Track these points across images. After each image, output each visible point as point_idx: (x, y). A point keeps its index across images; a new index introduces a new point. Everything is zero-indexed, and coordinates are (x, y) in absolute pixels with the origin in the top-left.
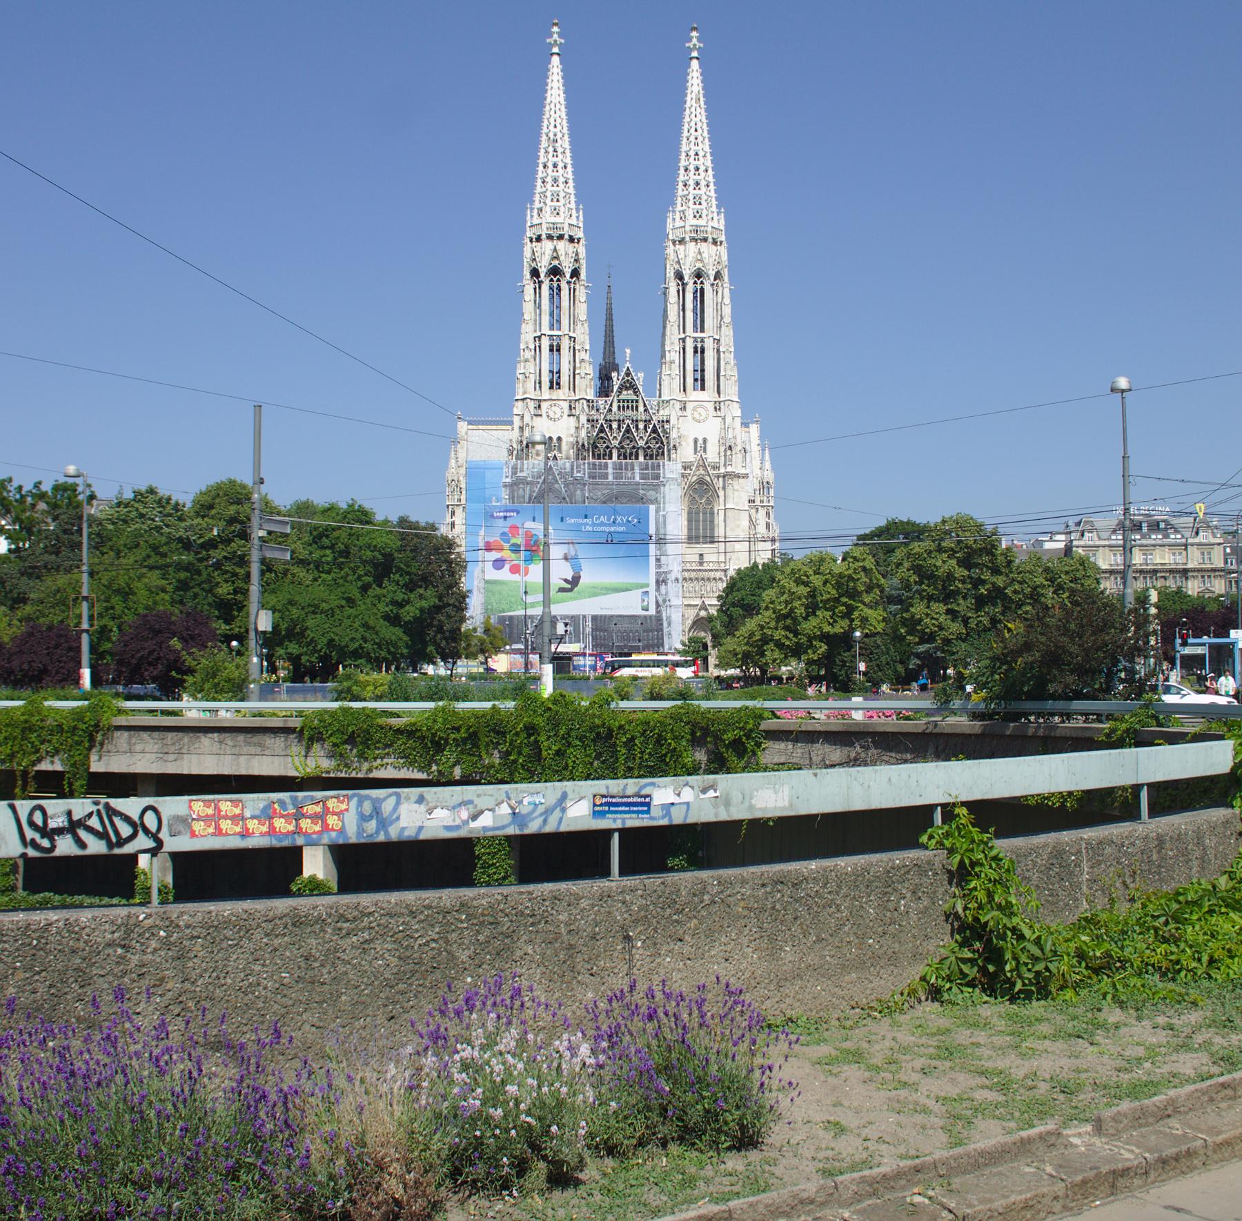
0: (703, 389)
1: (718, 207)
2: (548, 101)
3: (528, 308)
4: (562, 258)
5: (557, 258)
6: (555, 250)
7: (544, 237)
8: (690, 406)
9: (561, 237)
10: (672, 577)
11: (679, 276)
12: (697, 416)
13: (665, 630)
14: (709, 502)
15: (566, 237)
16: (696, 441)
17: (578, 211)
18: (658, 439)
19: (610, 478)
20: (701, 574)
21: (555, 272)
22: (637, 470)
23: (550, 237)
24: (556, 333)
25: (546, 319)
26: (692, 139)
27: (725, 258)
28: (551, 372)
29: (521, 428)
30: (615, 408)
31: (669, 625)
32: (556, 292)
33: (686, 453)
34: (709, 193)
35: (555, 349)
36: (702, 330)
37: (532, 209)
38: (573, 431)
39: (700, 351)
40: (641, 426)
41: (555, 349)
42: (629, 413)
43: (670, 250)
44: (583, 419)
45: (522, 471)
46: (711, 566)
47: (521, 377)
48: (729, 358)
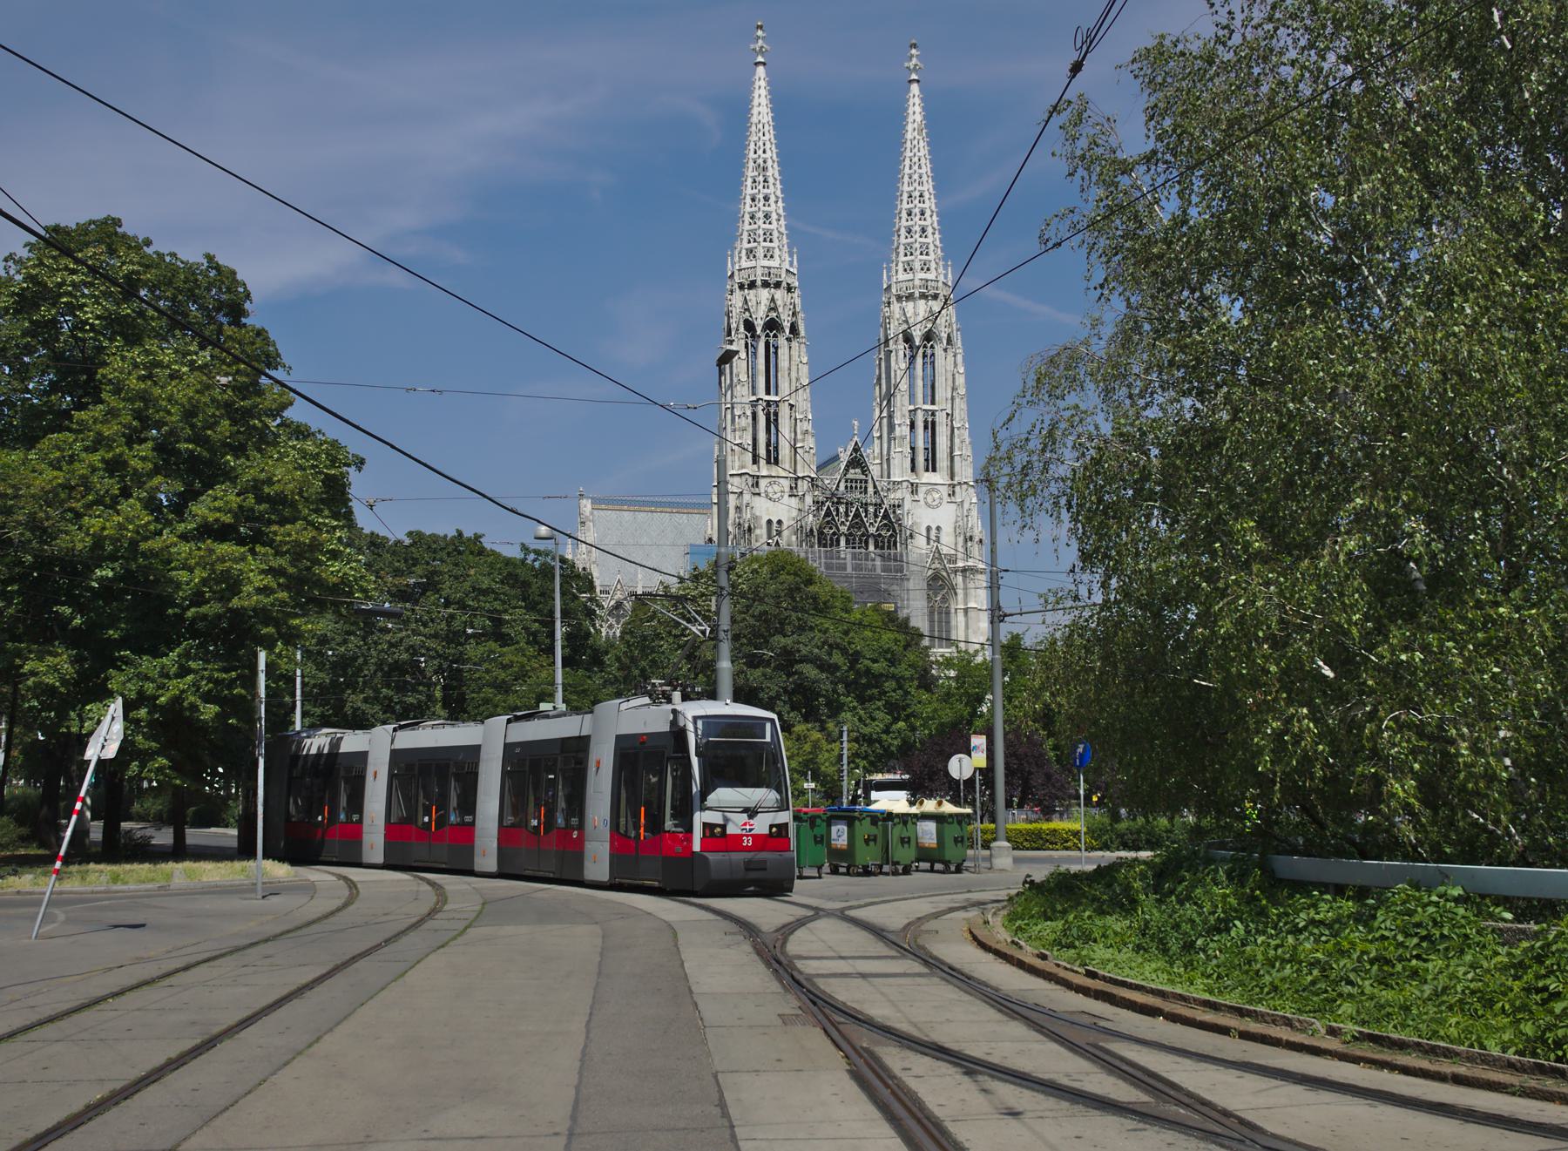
0: (934, 470)
1: (945, 259)
5: (774, 309)
6: (773, 300)
7: (759, 283)
8: (922, 490)
9: (778, 285)
12: (929, 500)
16: (929, 529)
17: (791, 255)
18: (889, 526)
19: (849, 570)
21: (773, 325)
23: (766, 284)
24: (772, 398)
26: (916, 177)
36: (933, 403)
38: (794, 513)
39: (931, 427)
40: (871, 509)
44: (809, 500)
48: (963, 435)
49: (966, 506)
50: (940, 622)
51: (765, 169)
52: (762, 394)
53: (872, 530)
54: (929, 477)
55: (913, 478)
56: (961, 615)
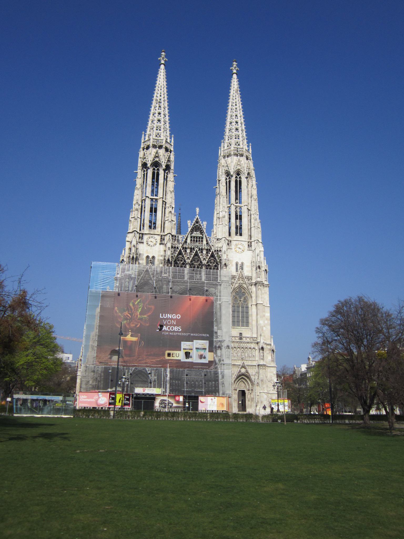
0: (241, 235)
1: (248, 143)
2: (158, 84)
3: (139, 181)
4: (161, 157)
5: (158, 157)
8: (233, 243)
9: (160, 147)
10: (225, 344)
11: (228, 174)
13: (220, 381)
14: (246, 300)
15: (164, 146)
17: (171, 138)
20: (242, 345)
21: (156, 164)
23: (154, 146)
24: (155, 197)
25: (149, 189)
27: (252, 167)
28: (150, 222)
29: (130, 249)
30: (189, 241)
31: (223, 377)
33: (232, 270)
34: (242, 134)
35: (153, 210)
37: (145, 135)
38: (162, 253)
39: (239, 217)
41: (153, 210)
42: (197, 244)
43: (222, 161)
44: (169, 245)
45: (129, 270)
46: (248, 340)
47: (132, 220)
49: (257, 251)
51: (160, 102)
52: (149, 194)
53: (204, 262)
54: (238, 238)
55: (230, 239)
56: (254, 307)
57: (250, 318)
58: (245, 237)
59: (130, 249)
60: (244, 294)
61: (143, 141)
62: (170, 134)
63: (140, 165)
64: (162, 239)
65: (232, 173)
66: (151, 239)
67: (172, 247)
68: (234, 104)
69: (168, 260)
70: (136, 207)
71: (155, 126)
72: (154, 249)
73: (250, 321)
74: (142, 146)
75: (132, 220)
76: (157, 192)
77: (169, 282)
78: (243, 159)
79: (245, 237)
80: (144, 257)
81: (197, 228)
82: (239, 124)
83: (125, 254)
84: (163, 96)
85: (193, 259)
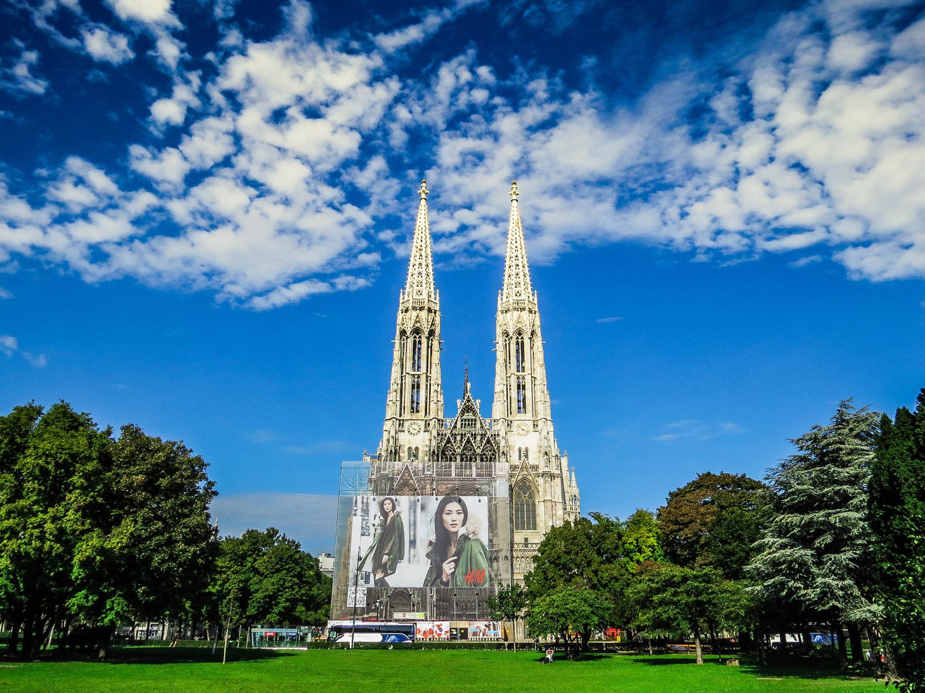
3: (396, 355)
8: (515, 424)
9: (421, 309)
10: (502, 555)
11: (506, 334)
14: (531, 497)
21: (417, 331)
22: (474, 468)
23: (414, 308)
25: (409, 364)
27: (538, 322)
29: (388, 440)
30: (459, 426)
32: (416, 346)
37: (404, 294)
38: (427, 443)
39: (521, 387)
41: (416, 387)
43: (500, 317)
44: (435, 433)
47: (390, 403)
50: (528, 511)
53: (479, 451)
54: (521, 416)
55: (510, 418)
57: (538, 518)
58: (529, 415)
59: (388, 440)
60: (529, 488)
61: (401, 301)
62: (435, 289)
63: (398, 334)
64: (427, 425)
65: (511, 334)
66: (414, 426)
67: (438, 434)
68: (514, 242)
69: (434, 452)
70: (394, 387)
71: (415, 281)
72: (416, 438)
73: (538, 522)
74: (400, 308)
75: (390, 403)
76: (419, 367)
77: (433, 480)
78: (525, 314)
79: (529, 415)
80: (406, 449)
81: (468, 409)
82: (520, 267)
83: (383, 448)
84: (424, 241)
85: (465, 448)
